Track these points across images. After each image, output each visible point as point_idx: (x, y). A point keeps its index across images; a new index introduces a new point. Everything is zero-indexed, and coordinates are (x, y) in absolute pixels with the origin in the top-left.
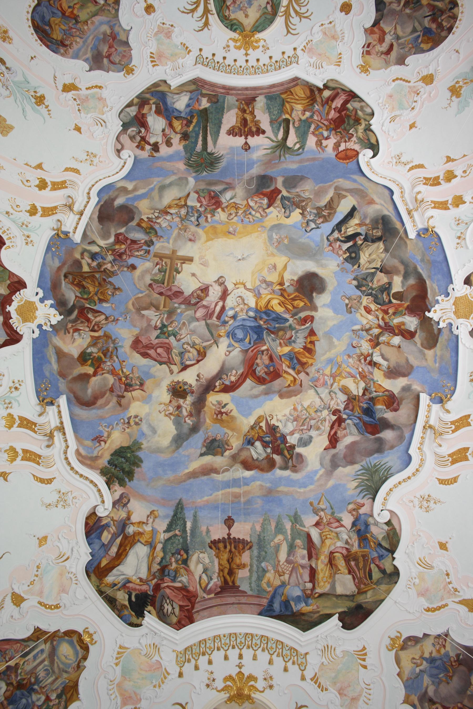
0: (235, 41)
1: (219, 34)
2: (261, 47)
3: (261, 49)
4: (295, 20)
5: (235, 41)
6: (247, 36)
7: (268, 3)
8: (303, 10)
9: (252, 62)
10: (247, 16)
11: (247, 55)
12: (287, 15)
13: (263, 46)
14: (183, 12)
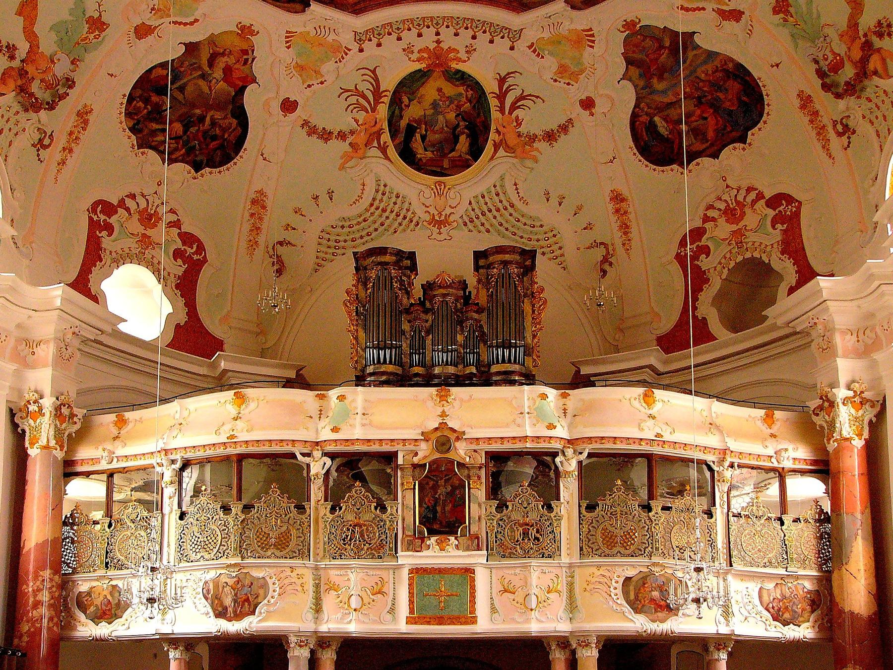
0: (459, 60)
1: (483, 67)
2: (416, 51)
3: (416, 50)
4: (366, 87)
5: (459, 60)
6: (438, 64)
7: (408, 106)
8: (353, 99)
9: (429, 35)
10: (440, 90)
11: (438, 42)
12: (377, 93)
13: (412, 52)
14: (537, 97)
